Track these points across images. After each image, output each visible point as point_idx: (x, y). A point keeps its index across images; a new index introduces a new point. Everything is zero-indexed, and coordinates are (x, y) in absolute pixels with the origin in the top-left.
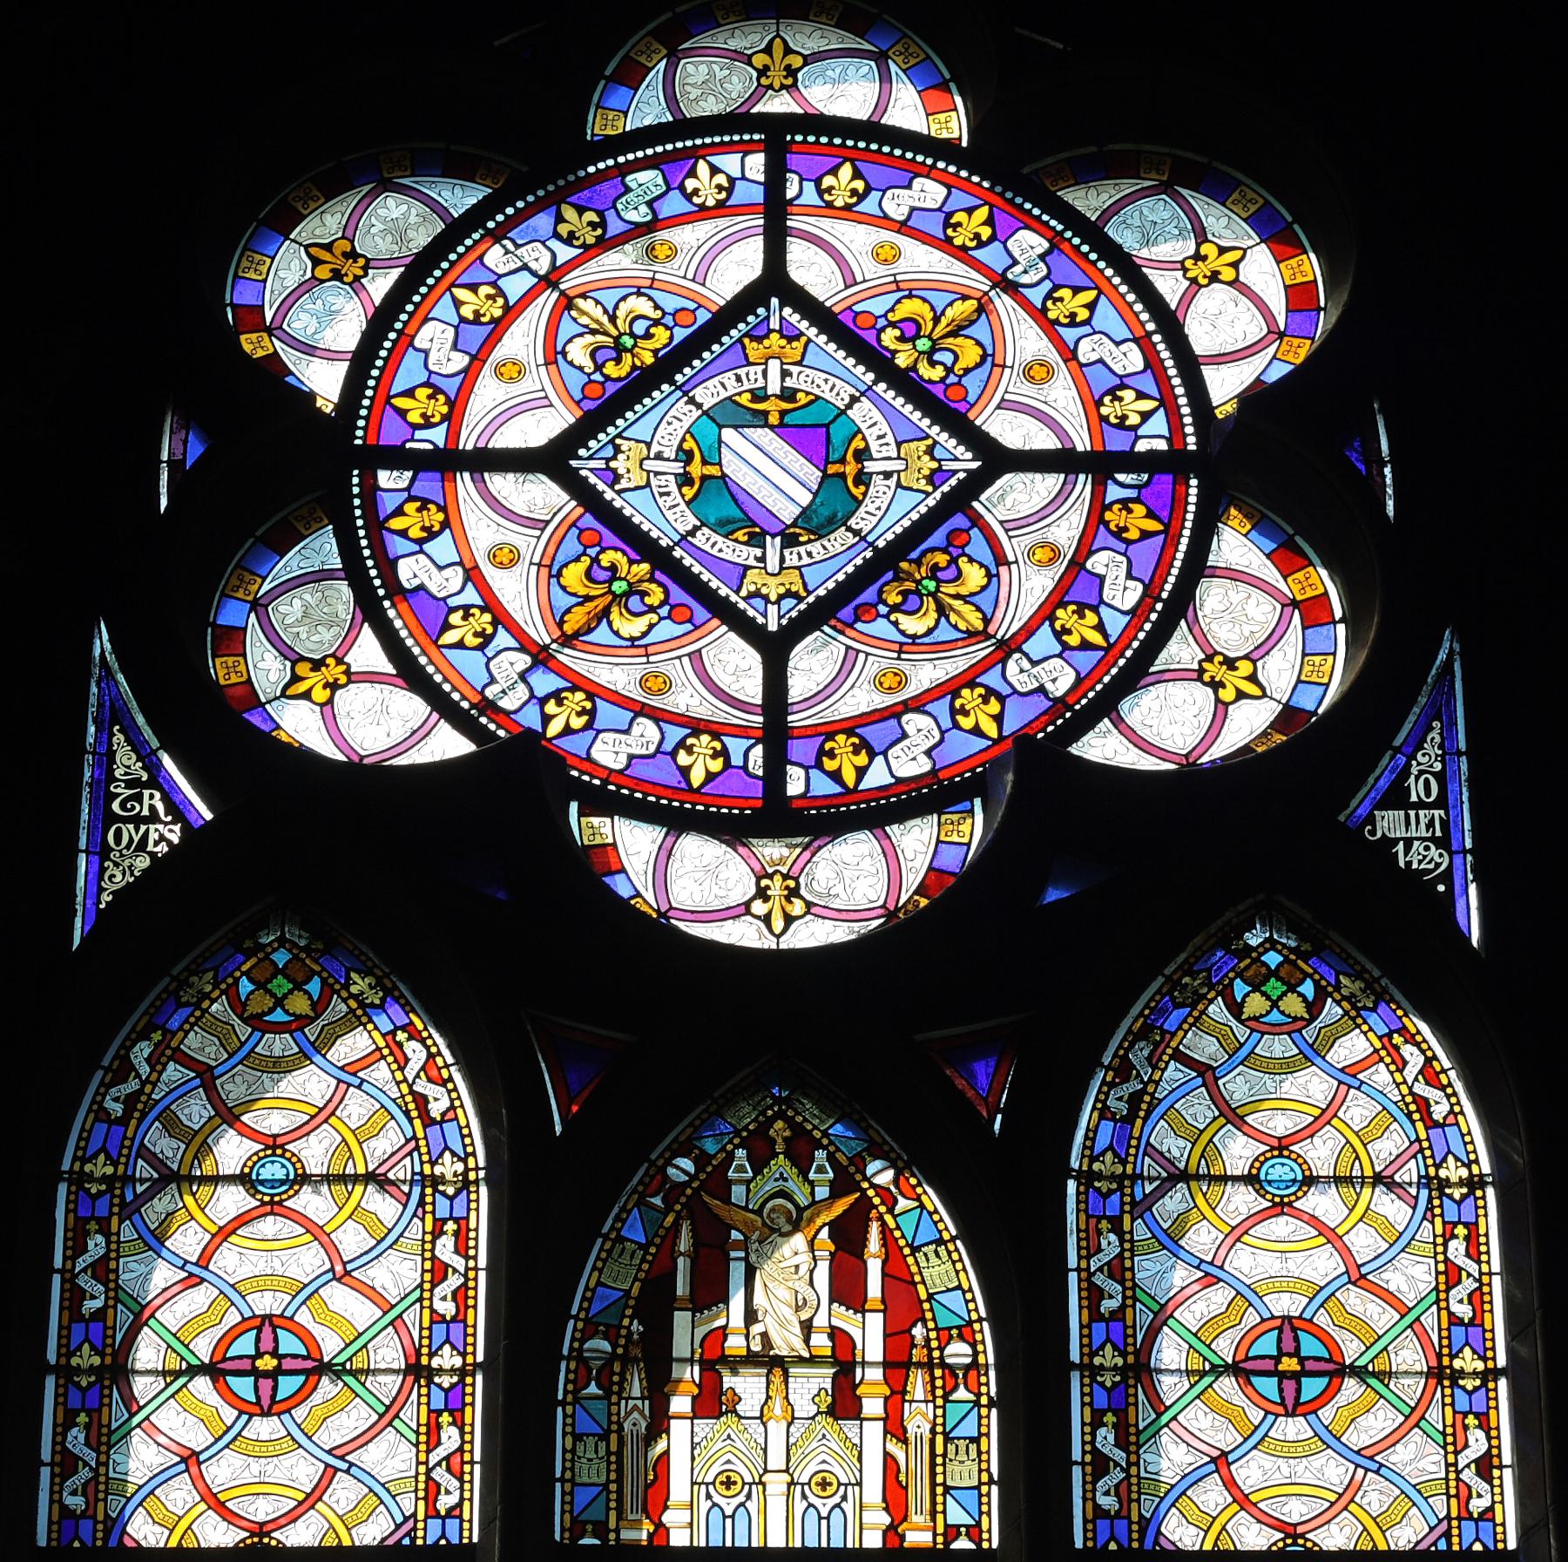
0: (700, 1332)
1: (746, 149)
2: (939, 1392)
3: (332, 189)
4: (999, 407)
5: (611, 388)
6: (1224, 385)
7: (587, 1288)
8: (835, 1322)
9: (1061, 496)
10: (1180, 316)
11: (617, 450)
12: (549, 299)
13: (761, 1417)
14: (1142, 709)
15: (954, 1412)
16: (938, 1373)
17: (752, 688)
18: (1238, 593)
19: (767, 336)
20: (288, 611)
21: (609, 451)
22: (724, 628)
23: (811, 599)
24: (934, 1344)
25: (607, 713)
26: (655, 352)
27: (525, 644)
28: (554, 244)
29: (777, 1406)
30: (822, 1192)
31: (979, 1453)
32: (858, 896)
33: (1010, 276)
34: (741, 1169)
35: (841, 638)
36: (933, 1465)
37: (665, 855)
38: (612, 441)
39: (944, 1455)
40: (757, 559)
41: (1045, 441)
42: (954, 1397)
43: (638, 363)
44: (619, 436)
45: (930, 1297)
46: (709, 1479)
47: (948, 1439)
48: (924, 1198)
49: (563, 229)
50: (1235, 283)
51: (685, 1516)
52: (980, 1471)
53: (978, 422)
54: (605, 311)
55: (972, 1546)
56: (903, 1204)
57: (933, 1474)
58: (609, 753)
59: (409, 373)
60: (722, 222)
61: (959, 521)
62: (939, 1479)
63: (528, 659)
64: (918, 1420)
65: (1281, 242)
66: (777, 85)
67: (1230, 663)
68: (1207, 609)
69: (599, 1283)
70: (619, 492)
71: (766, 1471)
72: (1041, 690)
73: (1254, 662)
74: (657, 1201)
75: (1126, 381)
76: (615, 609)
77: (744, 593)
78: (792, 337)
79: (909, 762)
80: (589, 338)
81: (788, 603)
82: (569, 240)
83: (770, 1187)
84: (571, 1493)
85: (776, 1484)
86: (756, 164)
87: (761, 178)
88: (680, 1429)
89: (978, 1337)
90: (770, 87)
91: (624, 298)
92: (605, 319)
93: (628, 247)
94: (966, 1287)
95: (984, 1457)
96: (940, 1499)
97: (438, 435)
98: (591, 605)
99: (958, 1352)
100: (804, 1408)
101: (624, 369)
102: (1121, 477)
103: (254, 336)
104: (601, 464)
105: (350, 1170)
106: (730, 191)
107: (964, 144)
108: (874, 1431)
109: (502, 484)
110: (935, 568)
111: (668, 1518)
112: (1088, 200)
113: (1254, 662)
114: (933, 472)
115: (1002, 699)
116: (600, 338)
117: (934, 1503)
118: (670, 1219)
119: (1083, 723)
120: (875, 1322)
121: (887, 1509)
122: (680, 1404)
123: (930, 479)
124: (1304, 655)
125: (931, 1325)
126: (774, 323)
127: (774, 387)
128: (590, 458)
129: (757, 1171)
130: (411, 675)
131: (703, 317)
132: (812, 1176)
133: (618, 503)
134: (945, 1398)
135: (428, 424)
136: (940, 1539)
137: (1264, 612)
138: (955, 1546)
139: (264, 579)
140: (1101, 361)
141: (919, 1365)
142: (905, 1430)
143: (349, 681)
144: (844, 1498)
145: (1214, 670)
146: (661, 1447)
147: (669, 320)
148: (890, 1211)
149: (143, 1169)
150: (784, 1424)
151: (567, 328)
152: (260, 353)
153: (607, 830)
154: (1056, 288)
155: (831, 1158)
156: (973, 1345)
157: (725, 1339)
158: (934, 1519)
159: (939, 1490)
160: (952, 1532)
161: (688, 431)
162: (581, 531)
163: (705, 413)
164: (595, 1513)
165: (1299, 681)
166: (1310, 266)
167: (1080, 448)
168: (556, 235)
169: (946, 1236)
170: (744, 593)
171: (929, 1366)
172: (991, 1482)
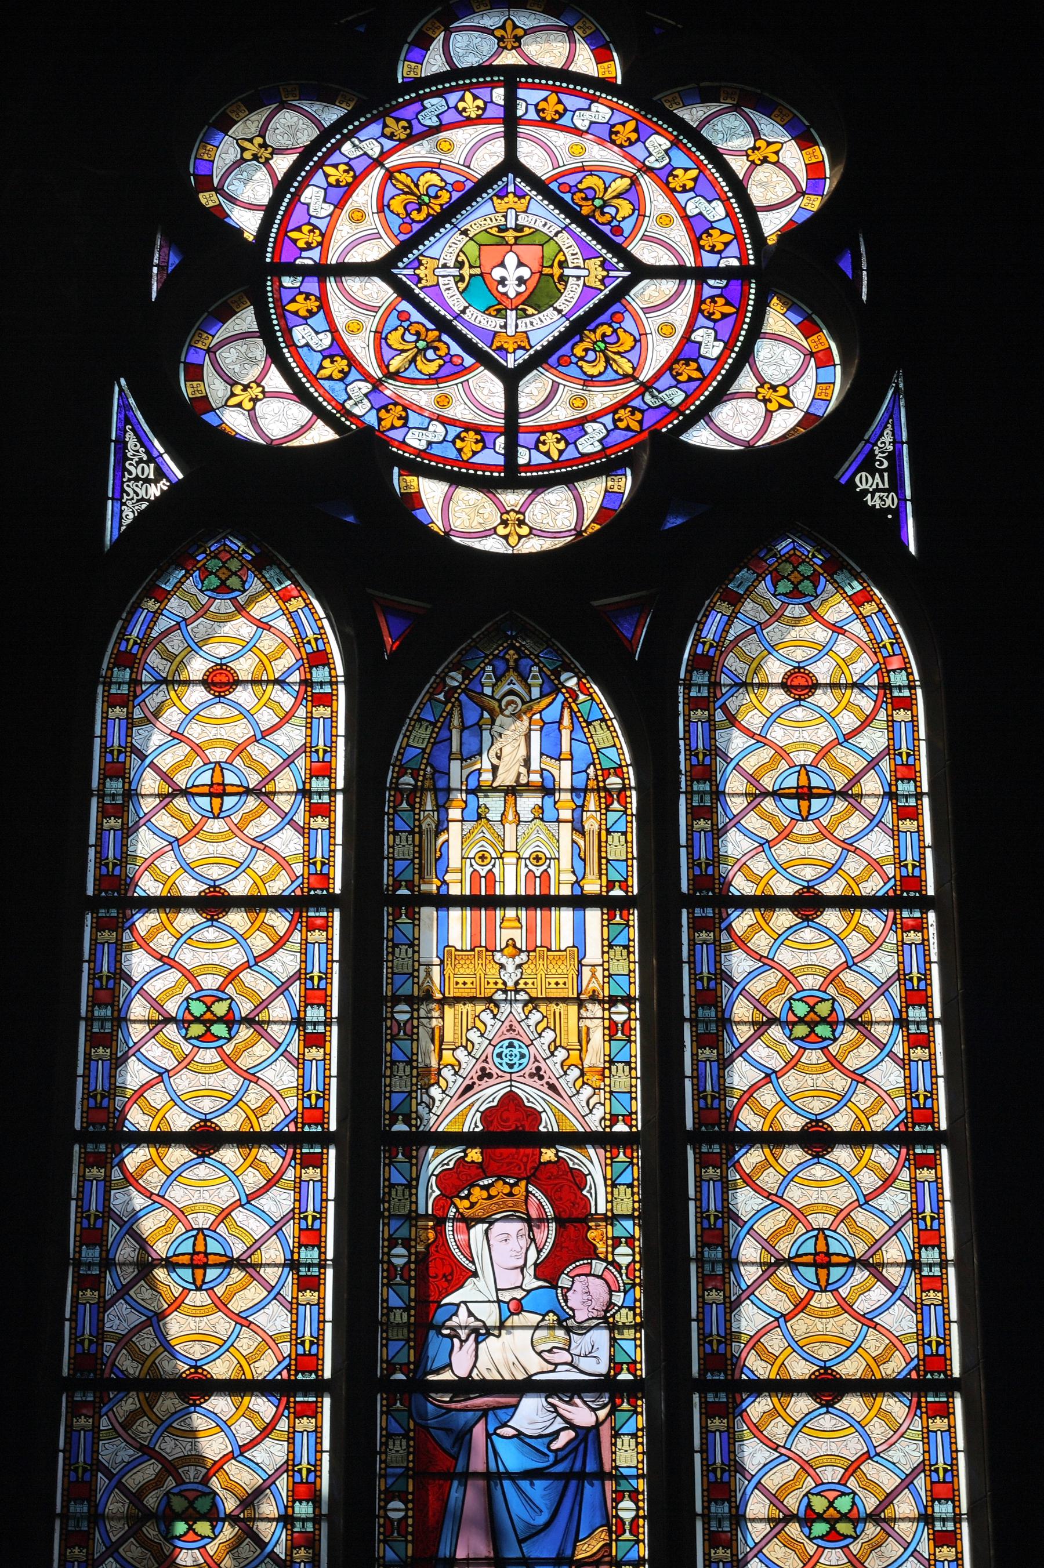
0: (466, 772)
1: (493, 85)
2: (603, 806)
3: (253, 107)
4: (641, 239)
5: (416, 227)
6: (771, 224)
7: (401, 747)
8: (543, 766)
9: (677, 294)
10: (744, 183)
11: (420, 263)
12: (378, 174)
13: (501, 821)
14: (723, 414)
15: (612, 817)
16: (603, 794)
17: (499, 403)
18: (780, 348)
19: (507, 196)
20: (228, 356)
21: (416, 264)
22: (482, 368)
23: (532, 352)
24: (600, 778)
25: (414, 419)
26: (441, 205)
27: (367, 377)
28: (383, 140)
29: (511, 816)
30: (536, 692)
31: (626, 842)
32: (559, 523)
33: (647, 163)
34: (489, 677)
35: (547, 374)
36: (600, 846)
37: (447, 500)
38: (417, 258)
39: (606, 842)
40: (501, 327)
41: (666, 260)
42: (612, 807)
43: (431, 212)
44: (421, 255)
45: (598, 750)
46: (472, 855)
47: (608, 832)
48: (594, 695)
49: (387, 131)
50: (777, 164)
51: (458, 876)
52: (627, 852)
53: (629, 249)
54: (413, 181)
55: (622, 893)
56: (582, 697)
57: (600, 851)
58: (416, 440)
59: (298, 216)
60: (480, 128)
61: (617, 307)
62: (603, 855)
63: (370, 386)
64: (591, 824)
65: (804, 141)
66: (509, 47)
67: (774, 388)
68: (761, 358)
69: (408, 745)
70: (421, 289)
71: (505, 851)
72: (665, 404)
73: (788, 387)
74: (441, 697)
75: (714, 225)
76: (418, 358)
77: (494, 347)
78: (520, 195)
79: (589, 445)
80: (403, 197)
81: (520, 352)
82: (391, 137)
83: (507, 688)
84: (393, 865)
86: (499, 95)
87: (502, 103)
88: (455, 829)
89: (626, 776)
90: (505, 48)
91: (423, 174)
92: (412, 186)
93: (425, 142)
94: (619, 746)
95: (629, 845)
96: (604, 867)
97: (315, 254)
98: (405, 355)
99: (614, 781)
100: (526, 815)
101: (422, 216)
102: (711, 282)
103: (207, 194)
104: (410, 272)
105: (265, 678)
106: (484, 110)
107: (619, 82)
108: (566, 829)
109: (353, 284)
110: (604, 335)
111: (448, 877)
112: (692, 115)
113: (788, 387)
114: (604, 277)
115: (642, 412)
116: (409, 196)
117: (600, 869)
118: (450, 705)
119: (689, 422)
120: (566, 766)
121: (574, 872)
122: (454, 813)
123: (602, 281)
124: (817, 383)
125: (598, 767)
126: (511, 188)
127: (511, 224)
128: (404, 268)
129: (498, 679)
130: (302, 395)
131: (469, 185)
132: (529, 681)
133: (422, 295)
134: (607, 809)
135: (309, 247)
136: (604, 889)
137: (792, 359)
138: (612, 893)
139: (213, 336)
140: (700, 214)
141: (592, 790)
142: (583, 827)
143: (265, 397)
144: (549, 866)
145: (764, 392)
146: (443, 838)
147: (449, 188)
148: (574, 701)
149: (146, 677)
150: (514, 825)
151: (390, 190)
152: (211, 204)
153: (415, 484)
154: (675, 169)
155: (541, 671)
156: (623, 779)
157: (480, 774)
158: (600, 878)
159: (604, 861)
161: (461, 251)
162: (399, 312)
163: (471, 239)
164: (407, 876)
165: (814, 398)
166: (821, 152)
167: (688, 265)
168: (383, 135)
169: (607, 717)
170: (494, 347)
171: (598, 790)
172: (633, 858)
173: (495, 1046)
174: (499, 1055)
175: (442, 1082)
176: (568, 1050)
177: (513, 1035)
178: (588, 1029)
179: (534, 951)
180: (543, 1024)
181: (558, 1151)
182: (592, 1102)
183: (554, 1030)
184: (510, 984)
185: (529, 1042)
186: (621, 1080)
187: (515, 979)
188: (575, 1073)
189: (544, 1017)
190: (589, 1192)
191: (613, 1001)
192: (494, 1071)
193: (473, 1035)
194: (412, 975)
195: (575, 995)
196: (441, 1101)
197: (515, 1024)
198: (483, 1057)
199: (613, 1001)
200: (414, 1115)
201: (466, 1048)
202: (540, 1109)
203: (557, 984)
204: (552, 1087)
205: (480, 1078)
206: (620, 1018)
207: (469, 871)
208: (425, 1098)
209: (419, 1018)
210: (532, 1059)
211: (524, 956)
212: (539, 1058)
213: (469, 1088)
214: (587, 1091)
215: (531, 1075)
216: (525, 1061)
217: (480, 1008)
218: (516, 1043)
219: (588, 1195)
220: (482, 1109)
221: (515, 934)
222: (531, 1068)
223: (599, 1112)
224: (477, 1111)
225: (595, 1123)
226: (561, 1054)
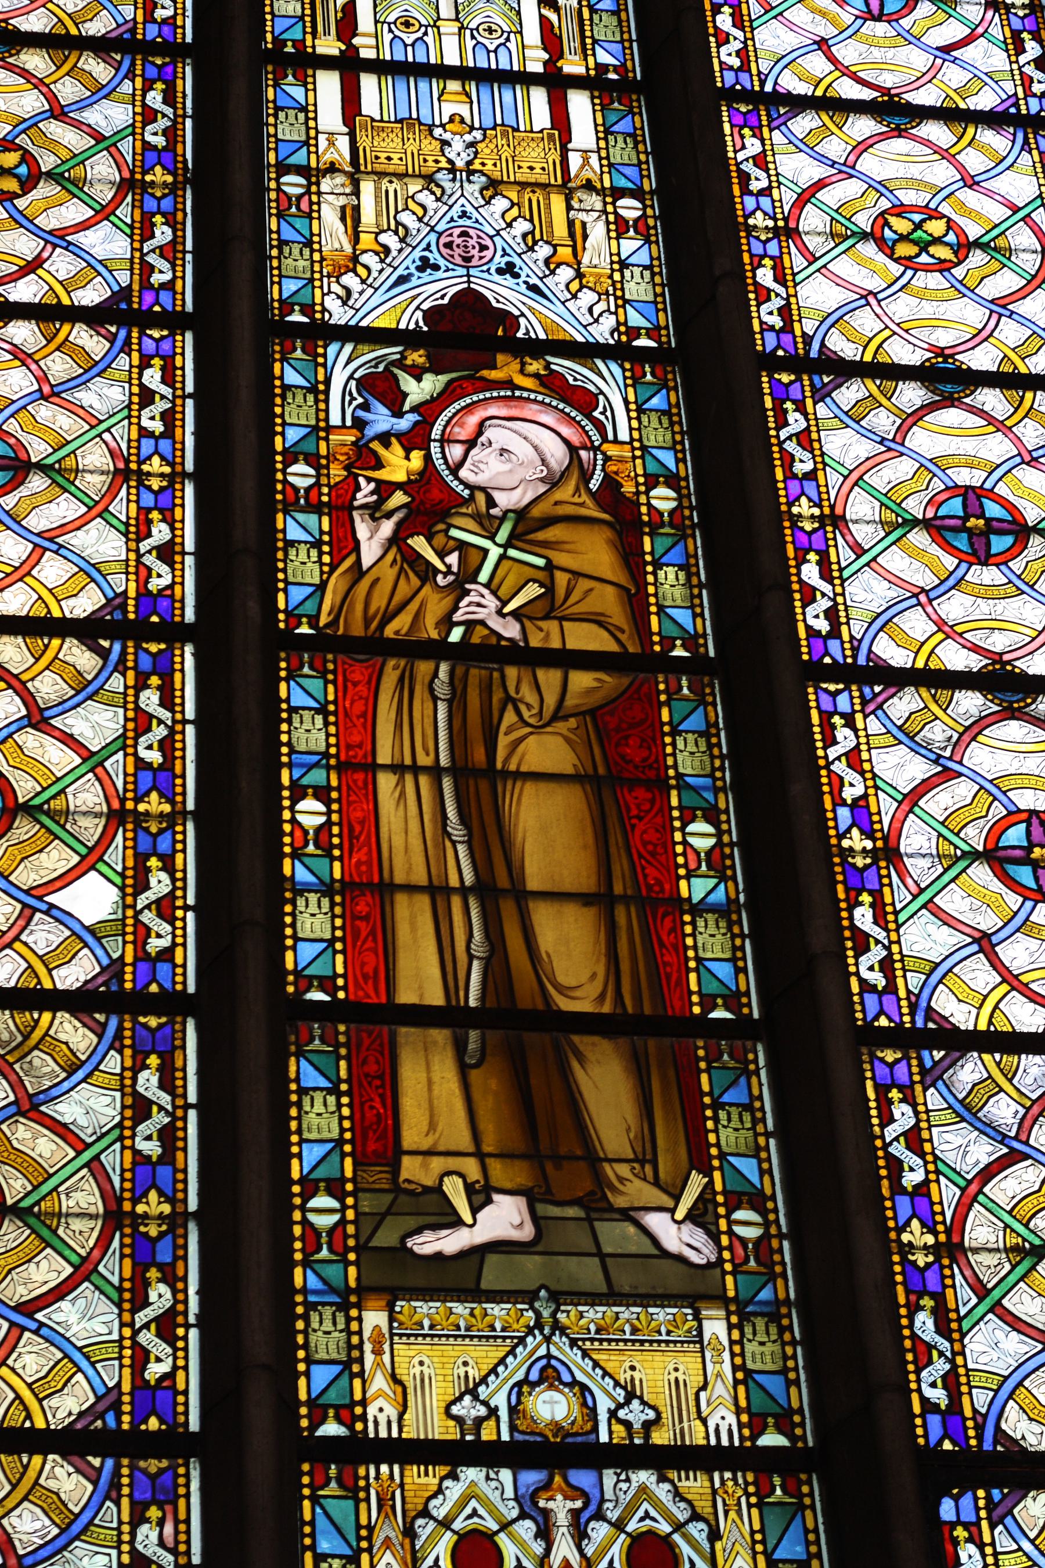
46: (390, 19)
47: (593, 10)
57: (582, 31)
62: (588, 34)
85: (449, 28)
121: (545, 49)
159: (589, 41)
160: (602, 68)
173: (440, 234)
174: (449, 245)
175: (360, 270)
176: (555, 247)
177: (468, 223)
178: (584, 224)
179: (494, 128)
180: (515, 212)
181: (549, 363)
182: (597, 311)
183: (531, 221)
184: (460, 163)
185: (492, 232)
186: (638, 288)
187: (465, 157)
188: (566, 273)
189: (513, 205)
190: (603, 413)
191: (618, 193)
192: (442, 262)
193: (406, 218)
194: (306, 143)
195: (560, 181)
196: (361, 293)
197: (469, 209)
198: (423, 245)
199: (618, 193)
200: (318, 308)
201: (396, 233)
202: (517, 313)
203: (531, 168)
204: (534, 288)
205: (421, 269)
206: (631, 215)
207: (388, 37)
208: (335, 288)
209: (319, 193)
210: (499, 253)
211: (478, 135)
212: (509, 250)
213: (402, 280)
214: (587, 297)
215: (500, 271)
216: (488, 254)
217: (414, 187)
218: (472, 232)
219: (602, 418)
220: (425, 306)
221: (464, 110)
222: (500, 261)
223: (608, 322)
224: (418, 308)
225: (603, 332)
226: (543, 251)
